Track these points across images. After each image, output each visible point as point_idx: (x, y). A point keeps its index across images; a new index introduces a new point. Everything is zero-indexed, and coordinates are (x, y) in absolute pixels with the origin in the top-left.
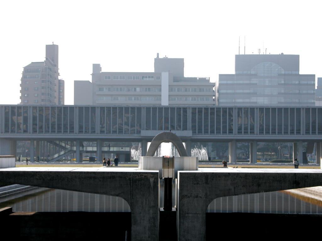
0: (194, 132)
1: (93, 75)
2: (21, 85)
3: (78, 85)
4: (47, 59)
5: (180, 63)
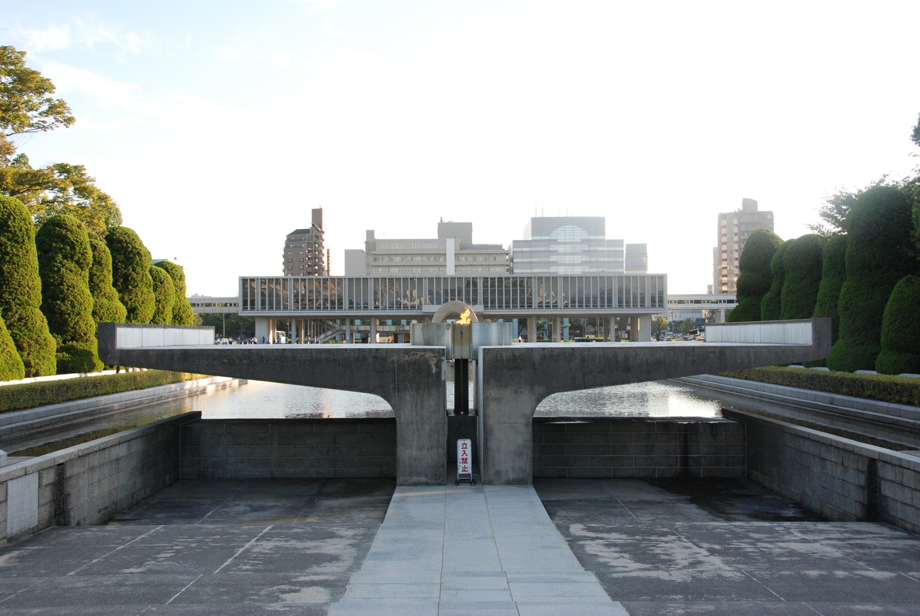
0: (486, 307)
1: (366, 243)
2: (284, 256)
3: (350, 255)
4: (313, 225)
5: (466, 228)
